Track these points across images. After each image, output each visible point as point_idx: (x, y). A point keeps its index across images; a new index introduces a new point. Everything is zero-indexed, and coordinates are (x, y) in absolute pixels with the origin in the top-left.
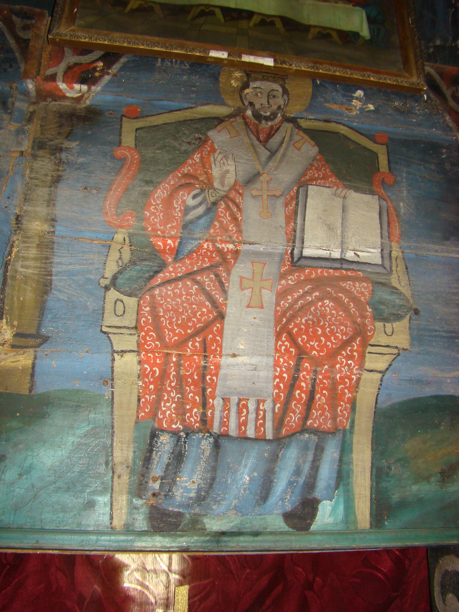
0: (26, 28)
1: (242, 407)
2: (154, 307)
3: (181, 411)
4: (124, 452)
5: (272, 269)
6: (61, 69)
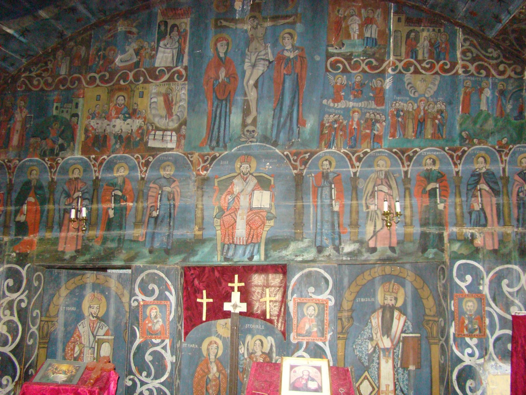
0: (191, 157)
1: (240, 239)
2: (223, 221)
3: (229, 240)
4: (219, 248)
5: (246, 211)
6: (200, 168)
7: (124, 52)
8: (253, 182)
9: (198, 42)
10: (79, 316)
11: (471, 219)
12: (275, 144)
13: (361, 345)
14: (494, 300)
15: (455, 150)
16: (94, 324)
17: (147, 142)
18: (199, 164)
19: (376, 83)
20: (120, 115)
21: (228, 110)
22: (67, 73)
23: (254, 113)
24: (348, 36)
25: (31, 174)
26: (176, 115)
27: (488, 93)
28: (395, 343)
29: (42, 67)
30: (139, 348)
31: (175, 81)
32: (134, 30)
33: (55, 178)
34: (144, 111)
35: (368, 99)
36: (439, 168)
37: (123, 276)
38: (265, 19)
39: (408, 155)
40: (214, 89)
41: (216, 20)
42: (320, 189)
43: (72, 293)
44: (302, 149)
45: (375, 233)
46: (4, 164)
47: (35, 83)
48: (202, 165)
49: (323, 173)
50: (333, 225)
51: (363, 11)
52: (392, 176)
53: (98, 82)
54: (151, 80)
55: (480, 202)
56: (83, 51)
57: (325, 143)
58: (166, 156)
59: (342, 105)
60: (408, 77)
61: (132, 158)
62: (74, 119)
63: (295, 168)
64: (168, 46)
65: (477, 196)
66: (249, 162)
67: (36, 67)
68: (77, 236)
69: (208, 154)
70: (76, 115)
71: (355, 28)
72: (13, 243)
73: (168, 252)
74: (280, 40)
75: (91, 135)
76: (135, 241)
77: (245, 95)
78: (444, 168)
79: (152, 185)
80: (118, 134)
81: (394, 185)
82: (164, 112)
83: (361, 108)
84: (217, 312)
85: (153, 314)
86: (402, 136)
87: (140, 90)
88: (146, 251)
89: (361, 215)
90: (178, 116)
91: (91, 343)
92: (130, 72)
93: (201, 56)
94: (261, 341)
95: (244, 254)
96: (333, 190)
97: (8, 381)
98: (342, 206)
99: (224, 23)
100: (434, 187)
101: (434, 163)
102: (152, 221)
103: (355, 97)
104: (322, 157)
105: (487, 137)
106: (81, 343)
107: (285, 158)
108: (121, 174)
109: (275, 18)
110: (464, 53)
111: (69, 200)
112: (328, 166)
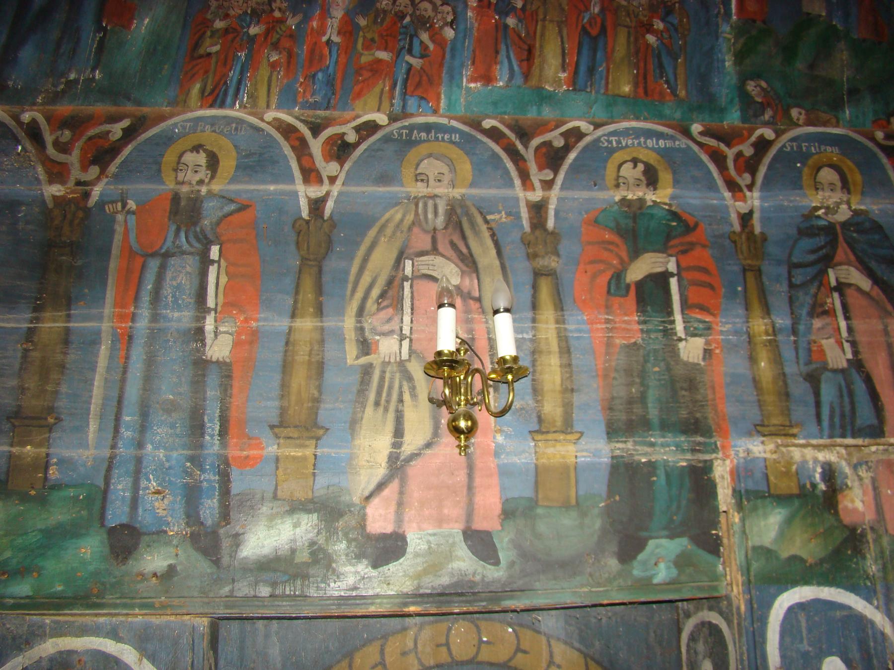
11: (818, 404)
15: (728, 138)
36: (673, 198)
39: (548, 144)
42: (154, 265)
45: (398, 466)
49: (176, 198)
50: (197, 427)
52: (479, 220)
55: (844, 334)
57: (202, 91)
63: (57, 173)
65: (830, 313)
78: (694, 200)
81: (487, 256)
86: (519, 80)
89: (331, 378)
96: (213, 271)
98: (249, 340)
100: (659, 270)
101: (651, 179)
104: (181, 136)
105: (836, 106)
107: (21, 134)
112: (203, 174)
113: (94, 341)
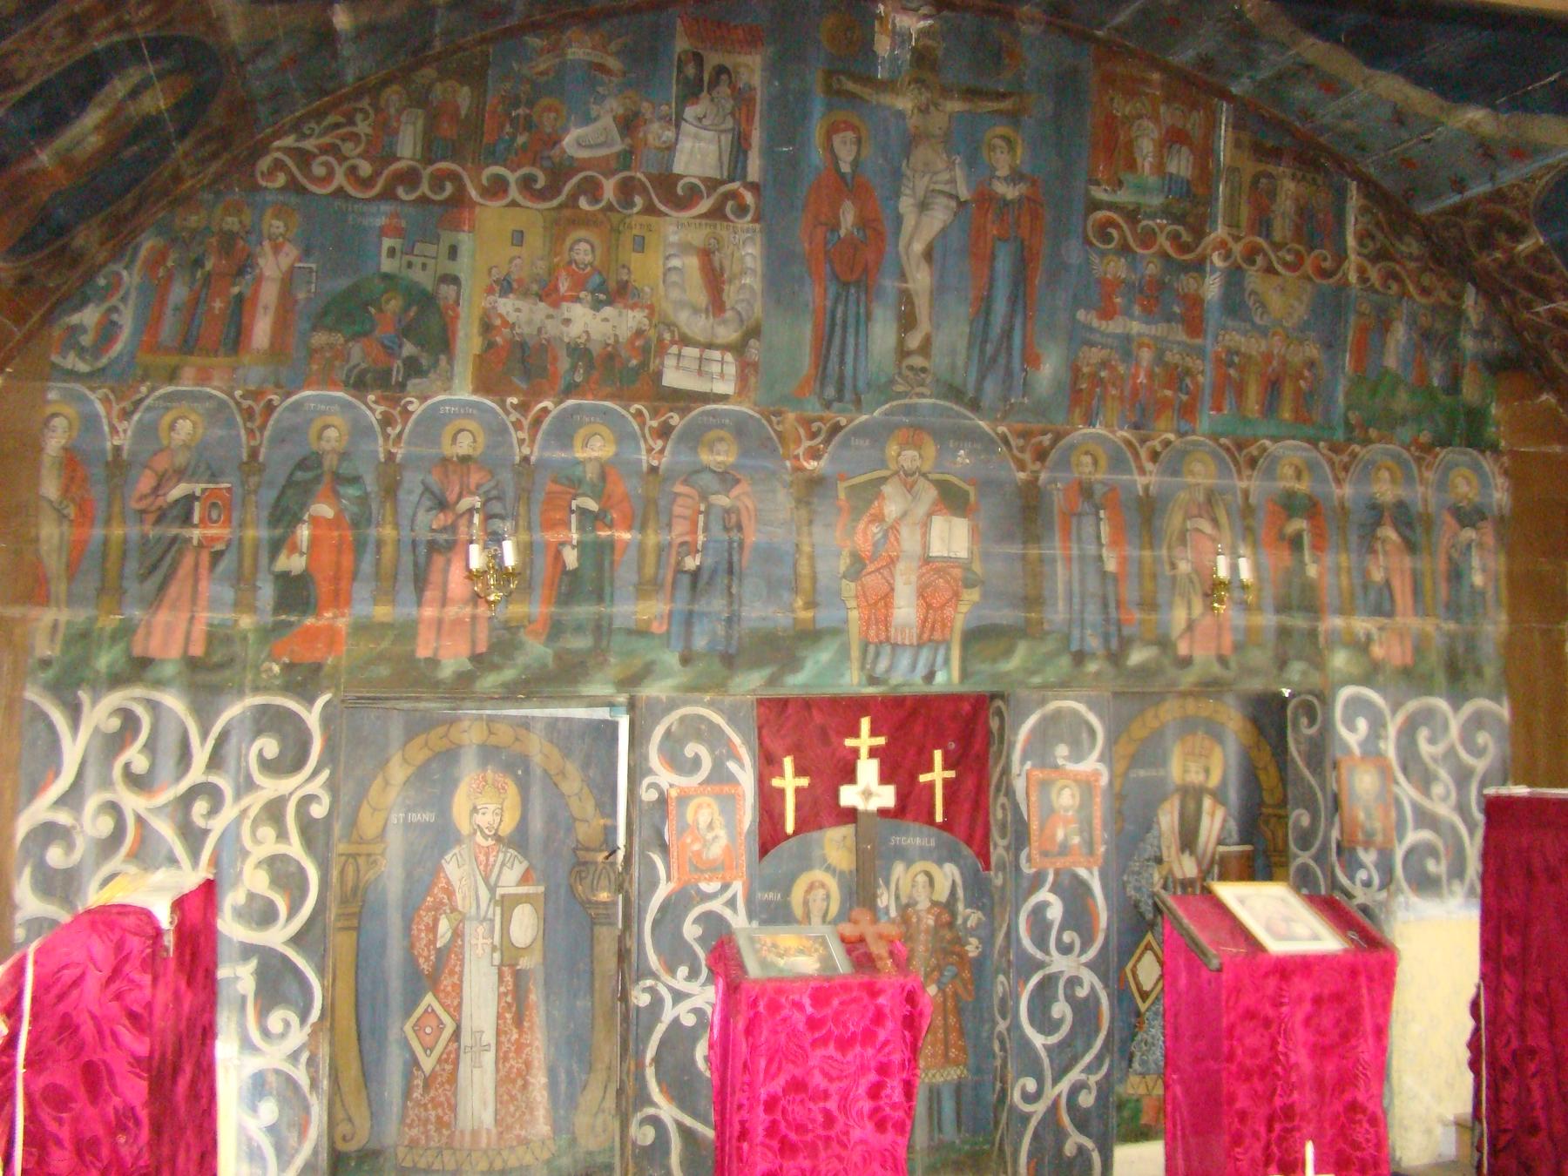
1: (903, 631)
2: (863, 586)
3: (877, 635)
4: (855, 653)
5: (915, 564)
6: (800, 451)
7: (587, 120)
8: (930, 494)
9: (788, 123)
10: (443, 836)
12: (975, 405)
13: (1139, 873)
14: (1405, 769)
16: (487, 855)
17: (659, 375)
18: (798, 442)
19: (1187, 283)
20: (582, 295)
21: (862, 310)
22: (418, 156)
23: (924, 326)
24: (1131, 165)
25: (320, 437)
26: (733, 308)
27: (1400, 333)
28: (1204, 867)
29: (337, 126)
30: (664, 908)
31: (728, 220)
32: (613, 63)
33: (400, 452)
34: (647, 289)
35: (1169, 318)
37: (560, 724)
38: (946, 92)
40: (826, 253)
41: (830, 74)
43: (421, 775)
44: (1035, 426)
45: (1190, 626)
46: (232, 404)
47: (319, 170)
48: (807, 444)
50: (1105, 605)
51: (1162, 109)
53: (514, 193)
54: (663, 208)
56: (464, 97)
58: (713, 414)
59: (1115, 326)
60: (1253, 278)
61: (624, 412)
62: (447, 291)
63: (1022, 466)
64: (706, 122)
66: (918, 446)
67: (318, 123)
68: (474, 618)
69: (821, 419)
70: (455, 280)
71: (1146, 148)
72: (269, 633)
73: (730, 661)
74: (985, 151)
75: (499, 339)
76: (641, 632)
77: (903, 276)
79: (679, 488)
80: (577, 345)
81: (1223, 519)
82: (702, 298)
83: (1155, 338)
84: (822, 809)
85: (703, 818)
87: (635, 232)
88: (671, 658)
90: (739, 314)
91: (483, 906)
92: (610, 173)
93: (793, 162)
94: (928, 874)
95: (914, 666)
97: (287, 1024)
98: (1123, 561)
99: (850, 86)
102: (685, 581)
103: (1144, 309)
106: (454, 909)
108: (595, 454)
109: (971, 93)
110: (1362, 238)
111: (441, 516)
112: (1090, 468)
113: (1054, 560)
